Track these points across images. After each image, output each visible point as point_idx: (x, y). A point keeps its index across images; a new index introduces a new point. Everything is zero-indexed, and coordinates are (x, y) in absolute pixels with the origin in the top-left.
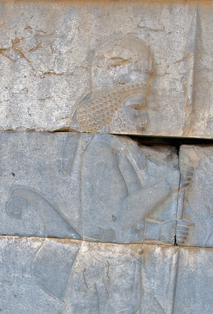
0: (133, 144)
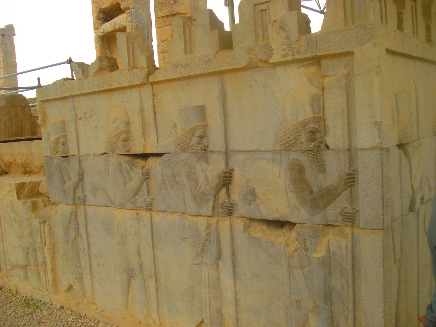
0: (127, 158)
